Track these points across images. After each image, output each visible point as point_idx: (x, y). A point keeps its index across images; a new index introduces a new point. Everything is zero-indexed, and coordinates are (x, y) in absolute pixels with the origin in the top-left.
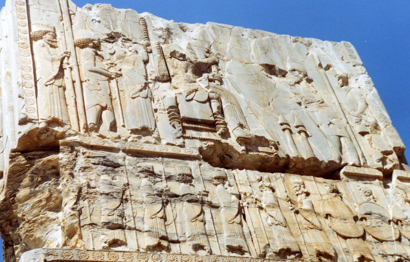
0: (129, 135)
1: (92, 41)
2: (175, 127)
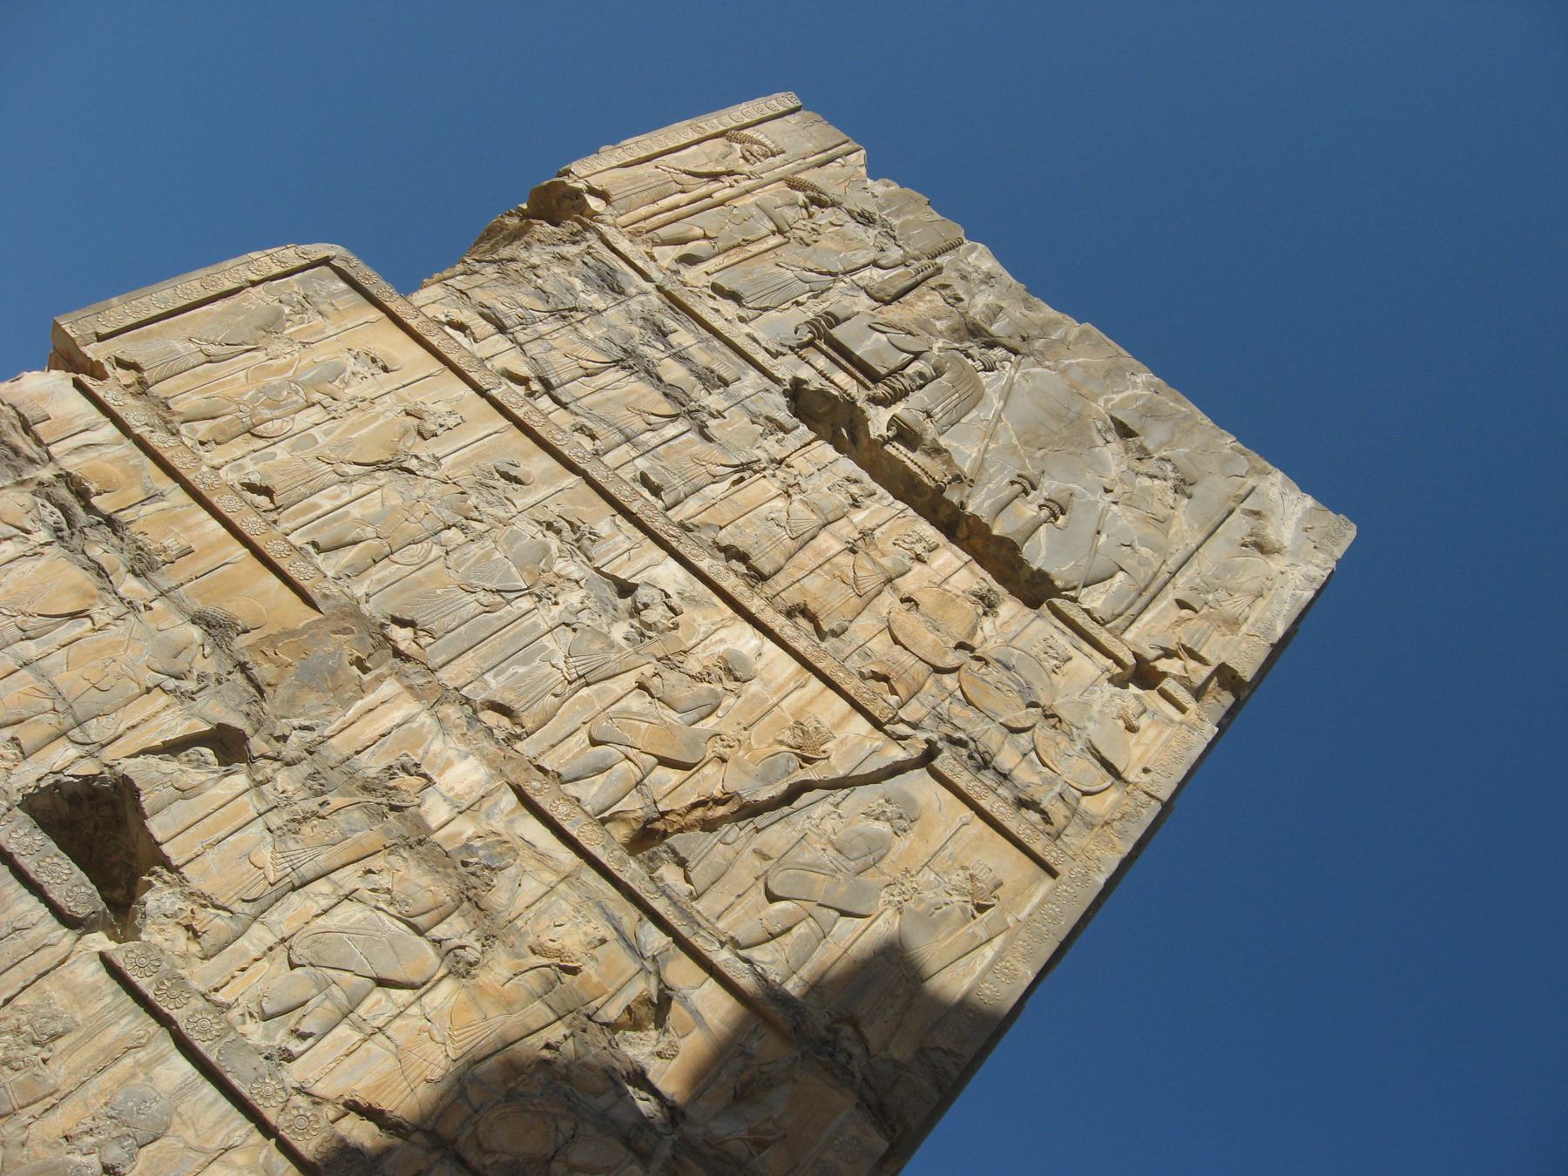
0: (700, 285)
1: (814, 188)
2: (796, 332)
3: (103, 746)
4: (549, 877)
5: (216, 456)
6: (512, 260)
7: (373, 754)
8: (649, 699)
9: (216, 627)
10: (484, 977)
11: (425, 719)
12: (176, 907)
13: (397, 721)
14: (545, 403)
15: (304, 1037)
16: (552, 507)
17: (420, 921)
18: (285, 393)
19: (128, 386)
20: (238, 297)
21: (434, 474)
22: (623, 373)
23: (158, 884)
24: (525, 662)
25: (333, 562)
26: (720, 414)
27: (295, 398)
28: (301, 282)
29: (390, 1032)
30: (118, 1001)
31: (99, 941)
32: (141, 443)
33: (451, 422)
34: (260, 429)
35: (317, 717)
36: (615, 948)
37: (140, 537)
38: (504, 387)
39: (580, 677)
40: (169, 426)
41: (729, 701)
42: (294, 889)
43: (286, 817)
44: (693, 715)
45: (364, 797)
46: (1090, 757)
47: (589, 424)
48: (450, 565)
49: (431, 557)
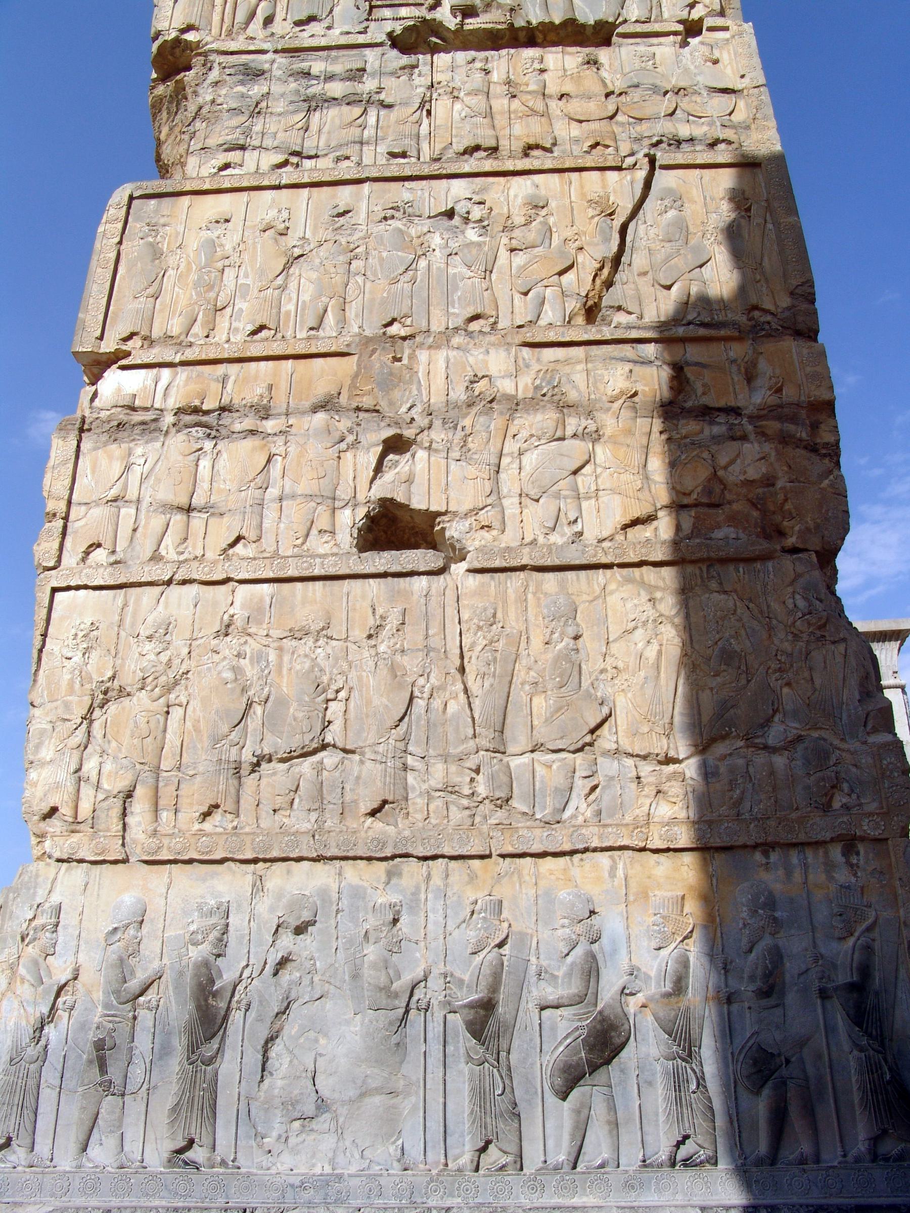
3: (355, 497)
4: (580, 367)
5: (220, 336)
6: (200, 108)
7: (453, 389)
8: (521, 253)
9: (325, 405)
10: (608, 431)
11: (452, 354)
12: (467, 525)
13: (444, 366)
14: (308, 163)
15: (576, 521)
16: (376, 209)
17: (559, 434)
18: (206, 278)
19: (142, 346)
20: (123, 256)
21: (312, 246)
22: (317, 114)
23: (447, 525)
24: (456, 288)
25: (328, 328)
26: (380, 90)
27: (213, 275)
28: (136, 220)
29: (601, 487)
30: (497, 580)
31: (457, 569)
32: (184, 363)
33: (285, 215)
34: (219, 305)
35: (408, 399)
36: (637, 369)
37: (244, 402)
38: (284, 175)
39: (485, 272)
40: (184, 344)
41: (551, 220)
42: (498, 472)
43: (457, 449)
44: (547, 241)
45: (474, 410)
46: (714, 94)
47: (338, 154)
48: (373, 279)
49: (361, 284)
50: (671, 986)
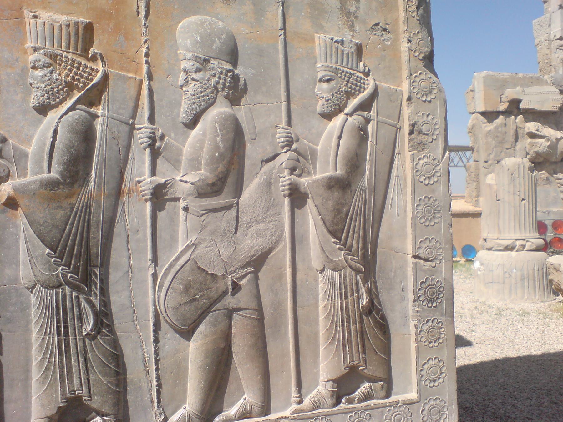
50: (59, 169)
